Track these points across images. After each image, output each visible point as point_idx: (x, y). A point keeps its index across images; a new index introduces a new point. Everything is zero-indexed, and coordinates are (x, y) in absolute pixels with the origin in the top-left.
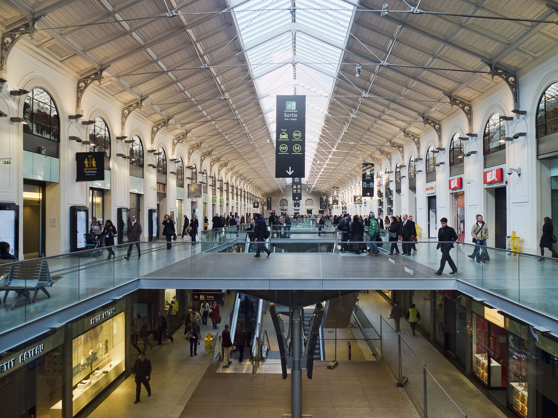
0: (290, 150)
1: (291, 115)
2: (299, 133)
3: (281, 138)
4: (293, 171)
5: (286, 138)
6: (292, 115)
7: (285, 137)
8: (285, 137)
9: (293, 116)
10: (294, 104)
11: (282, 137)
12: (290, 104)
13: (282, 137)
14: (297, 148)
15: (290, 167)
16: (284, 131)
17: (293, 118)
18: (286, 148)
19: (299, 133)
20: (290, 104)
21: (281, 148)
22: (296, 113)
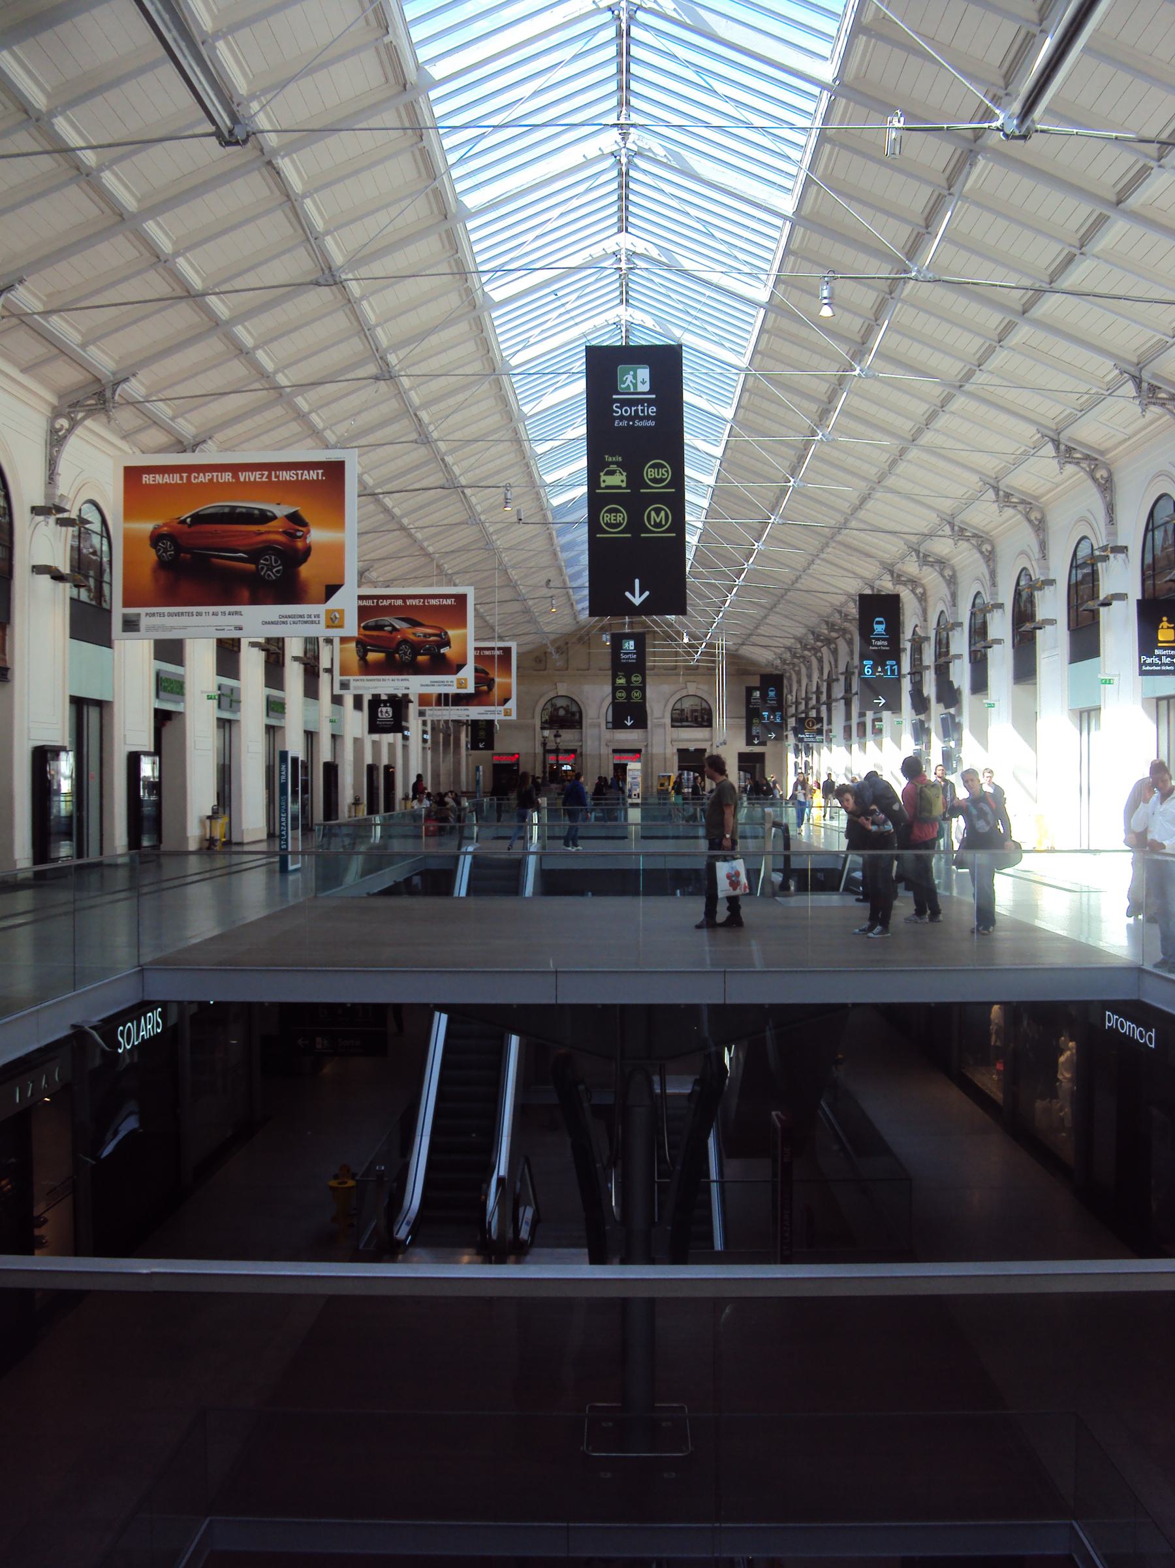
1: (636, 411)
3: (603, 485)
4: (647, 593)
5: (618, 483)
6: (640, 408)
7: (616, 480)
8: (616, 480)
9: (643, 411)
10: (644, 373)
12: (632, 373)
13: (608, 480)
15: (637, 581)
16: (613, 463)
17: (641, 419)
18: (622, 517)
20: (632, 373)
21: (605, 518)
22: (650, 402)
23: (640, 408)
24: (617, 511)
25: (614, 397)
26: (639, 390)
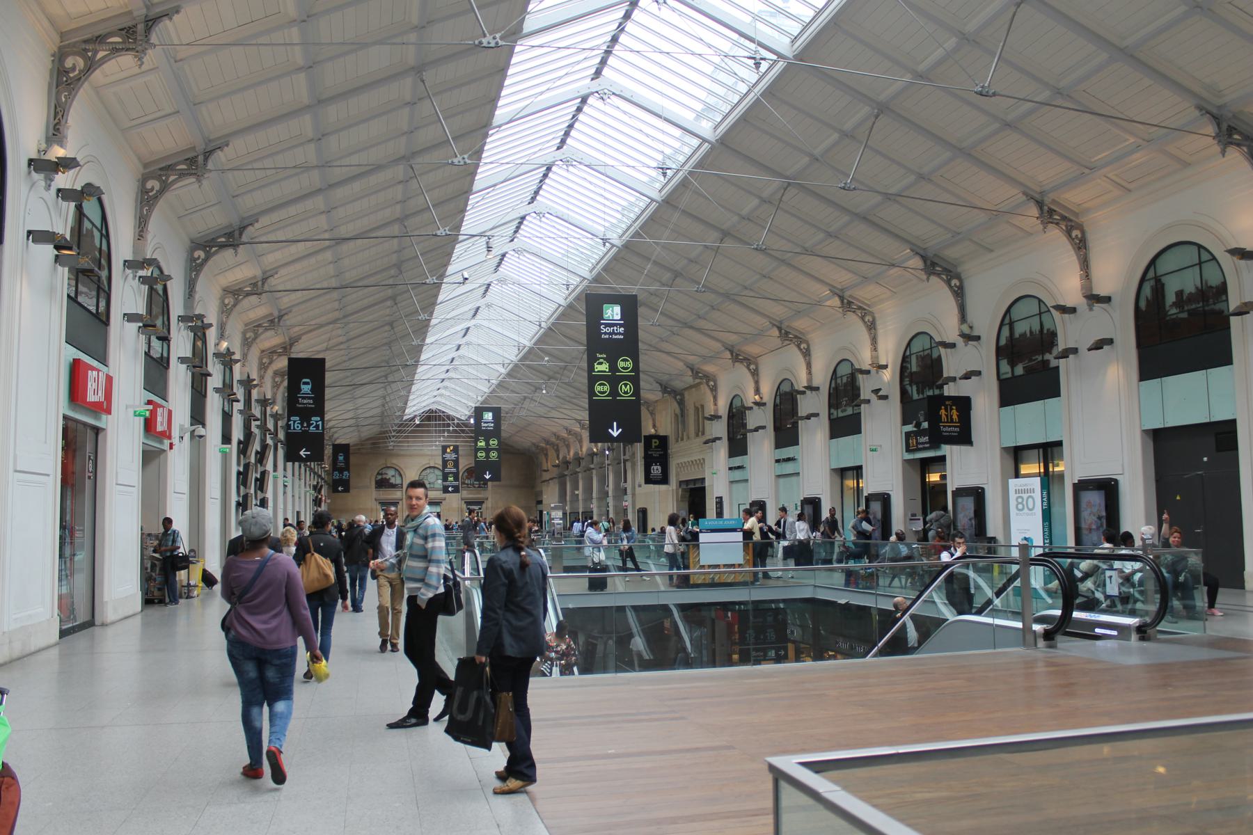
0: (614, 392)
1: (613, 330)
2: (628, 361)
3: (596, 370)
6: (615, 328)
7: (602, 368)
8: (602, 368)
9: (617, 330)
11: (598, 368)
13: (598, 368)
14: (625, 389)
15: (615, 423)
16: (601, 358)
17: (616, 334)
18: (607, 388)
19: (628, 361)
21: (598, 388)
22: (621, 326)
23: (615, 328)
24: (604, 385)
25: (602, 322)
26: (615, 318)
